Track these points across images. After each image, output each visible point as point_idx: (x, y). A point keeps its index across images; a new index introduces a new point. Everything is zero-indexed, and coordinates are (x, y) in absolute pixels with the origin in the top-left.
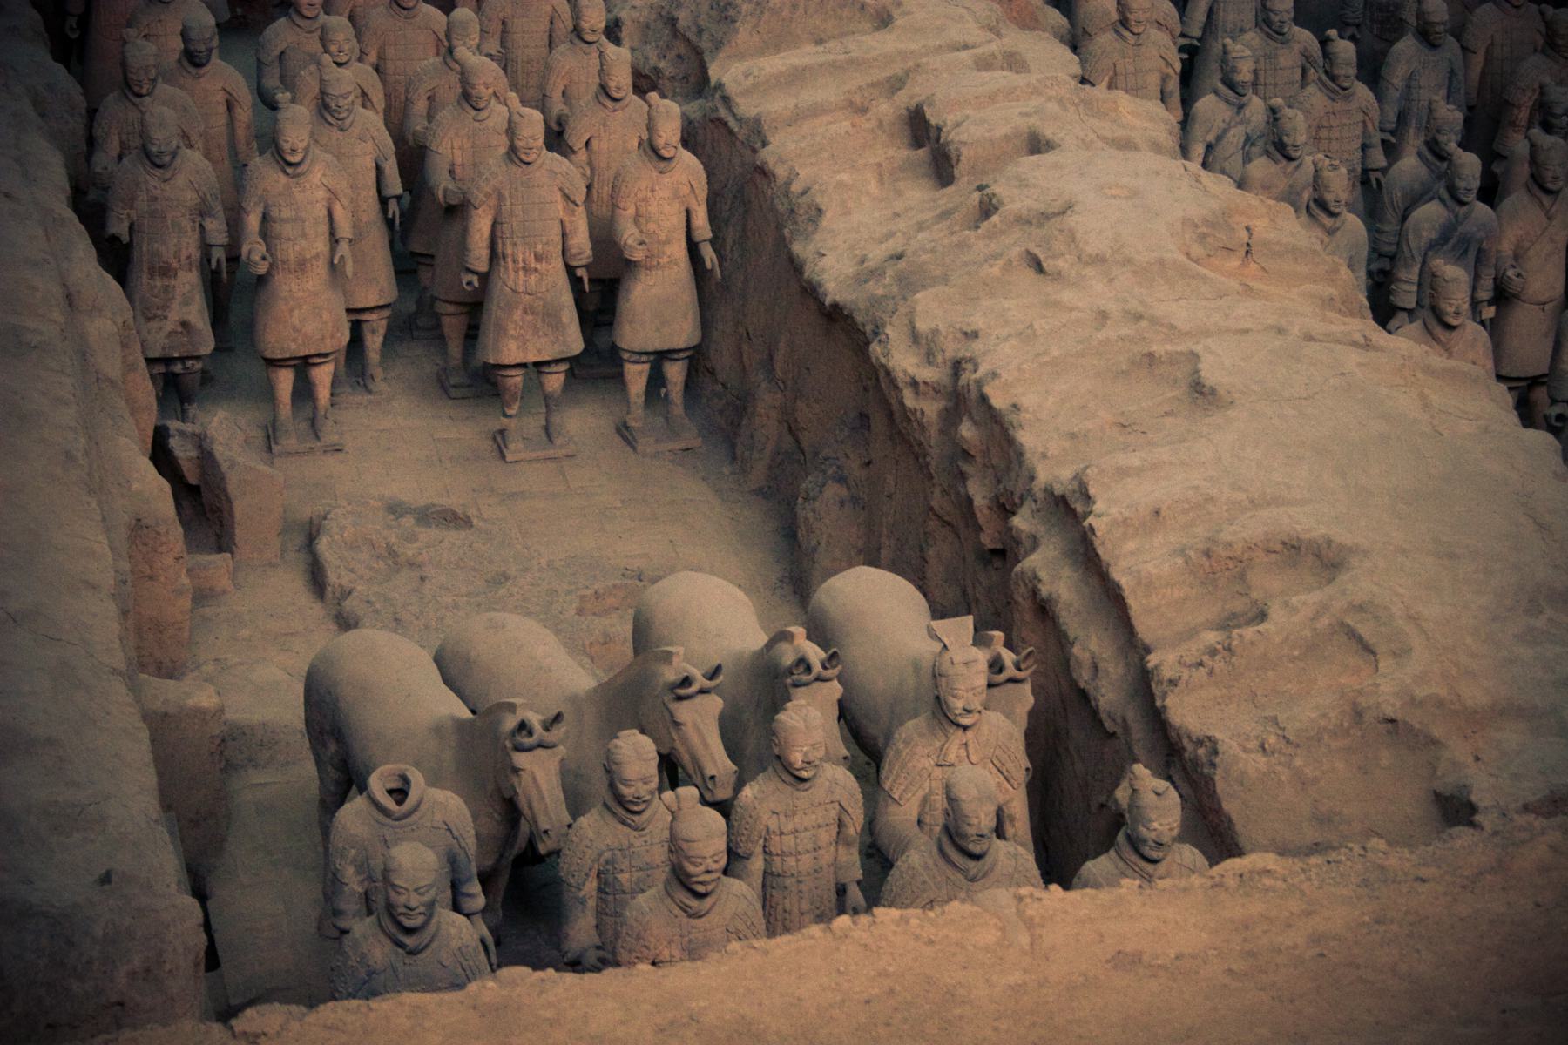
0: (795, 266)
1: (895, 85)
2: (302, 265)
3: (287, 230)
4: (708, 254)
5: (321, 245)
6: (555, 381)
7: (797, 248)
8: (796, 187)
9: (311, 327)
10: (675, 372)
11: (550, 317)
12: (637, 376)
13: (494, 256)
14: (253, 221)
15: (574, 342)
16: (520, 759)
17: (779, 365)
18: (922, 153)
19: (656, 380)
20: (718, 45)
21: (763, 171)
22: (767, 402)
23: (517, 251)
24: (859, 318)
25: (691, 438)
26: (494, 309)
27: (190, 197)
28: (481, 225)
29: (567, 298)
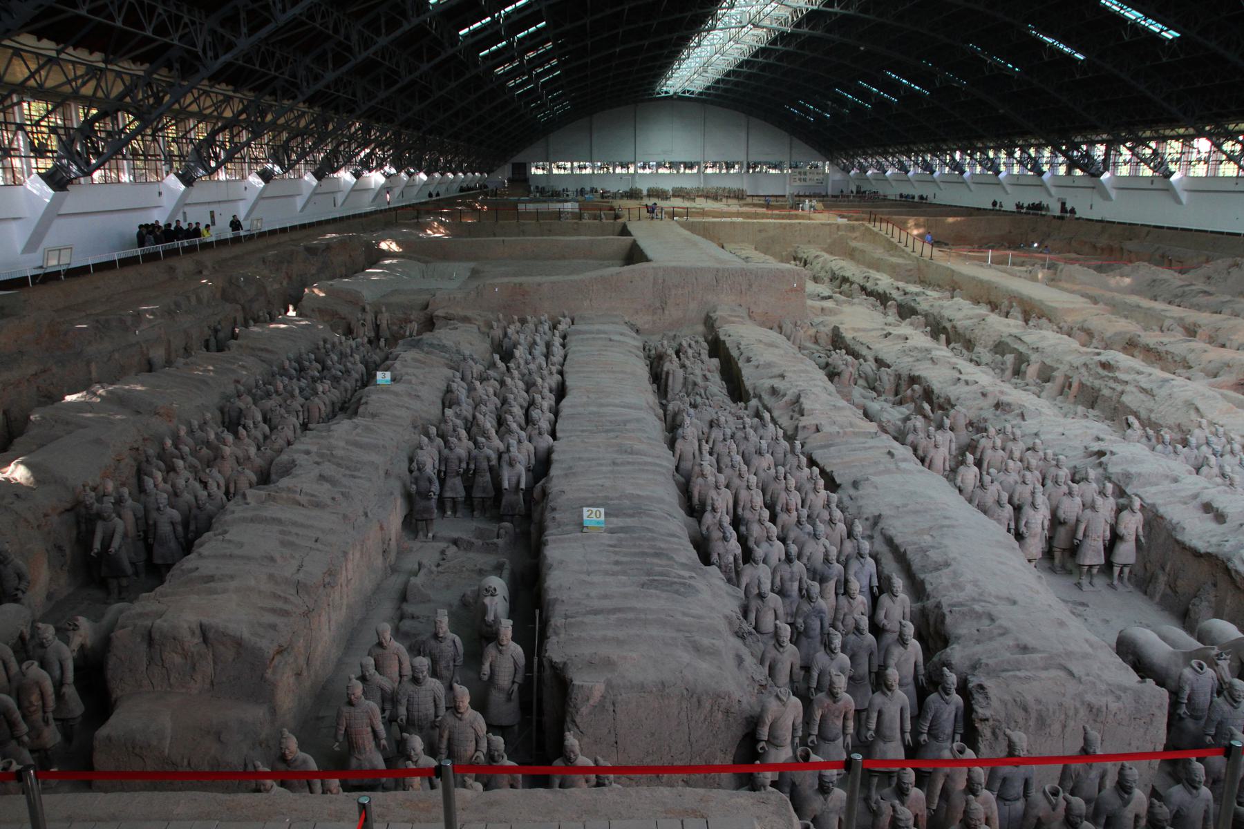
0: (1178, 542)
1: (1195, 496)
2: (1035, 536)
3: (1033, 526)
4: (1142, 539)
5: (1040, 529)
6: (1095, 571)
7: (1179, 538)
8: (1174, 521)
9: (1034, 552)
10: (1126, 570)
11: (1099, 553)
12: (1116, 570)
13: (1085, 535)
14: (1023, 523)
15: (1103, 561)
16: (1219, 662)
17: (1167, 569)
18: (1211, 515)
19: (1121, 572)
20: (1127, 485)
21: (1162, 517)
22: (1162, 579)
23: (1092, 534)
24: (1220, 557)
25: (1131, 588)
26: (1083, 549)
27: (1007, 515)
28: (1082, 528)
29: (1102, 548)
